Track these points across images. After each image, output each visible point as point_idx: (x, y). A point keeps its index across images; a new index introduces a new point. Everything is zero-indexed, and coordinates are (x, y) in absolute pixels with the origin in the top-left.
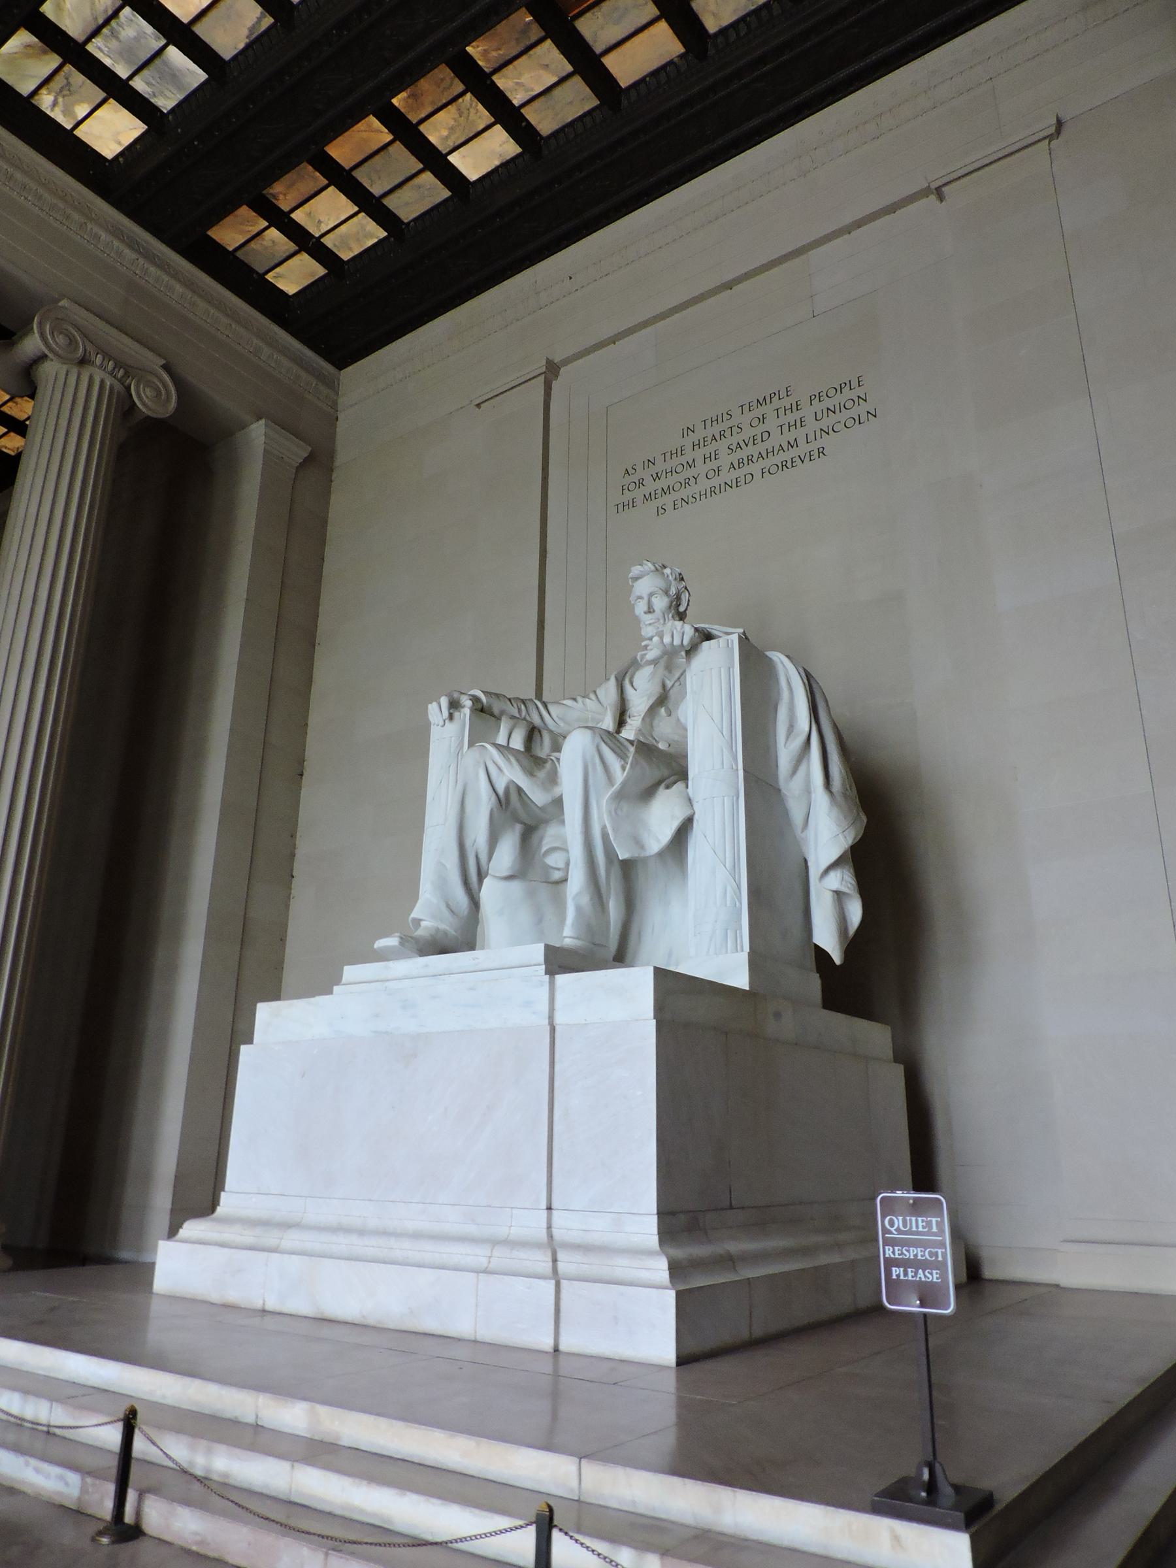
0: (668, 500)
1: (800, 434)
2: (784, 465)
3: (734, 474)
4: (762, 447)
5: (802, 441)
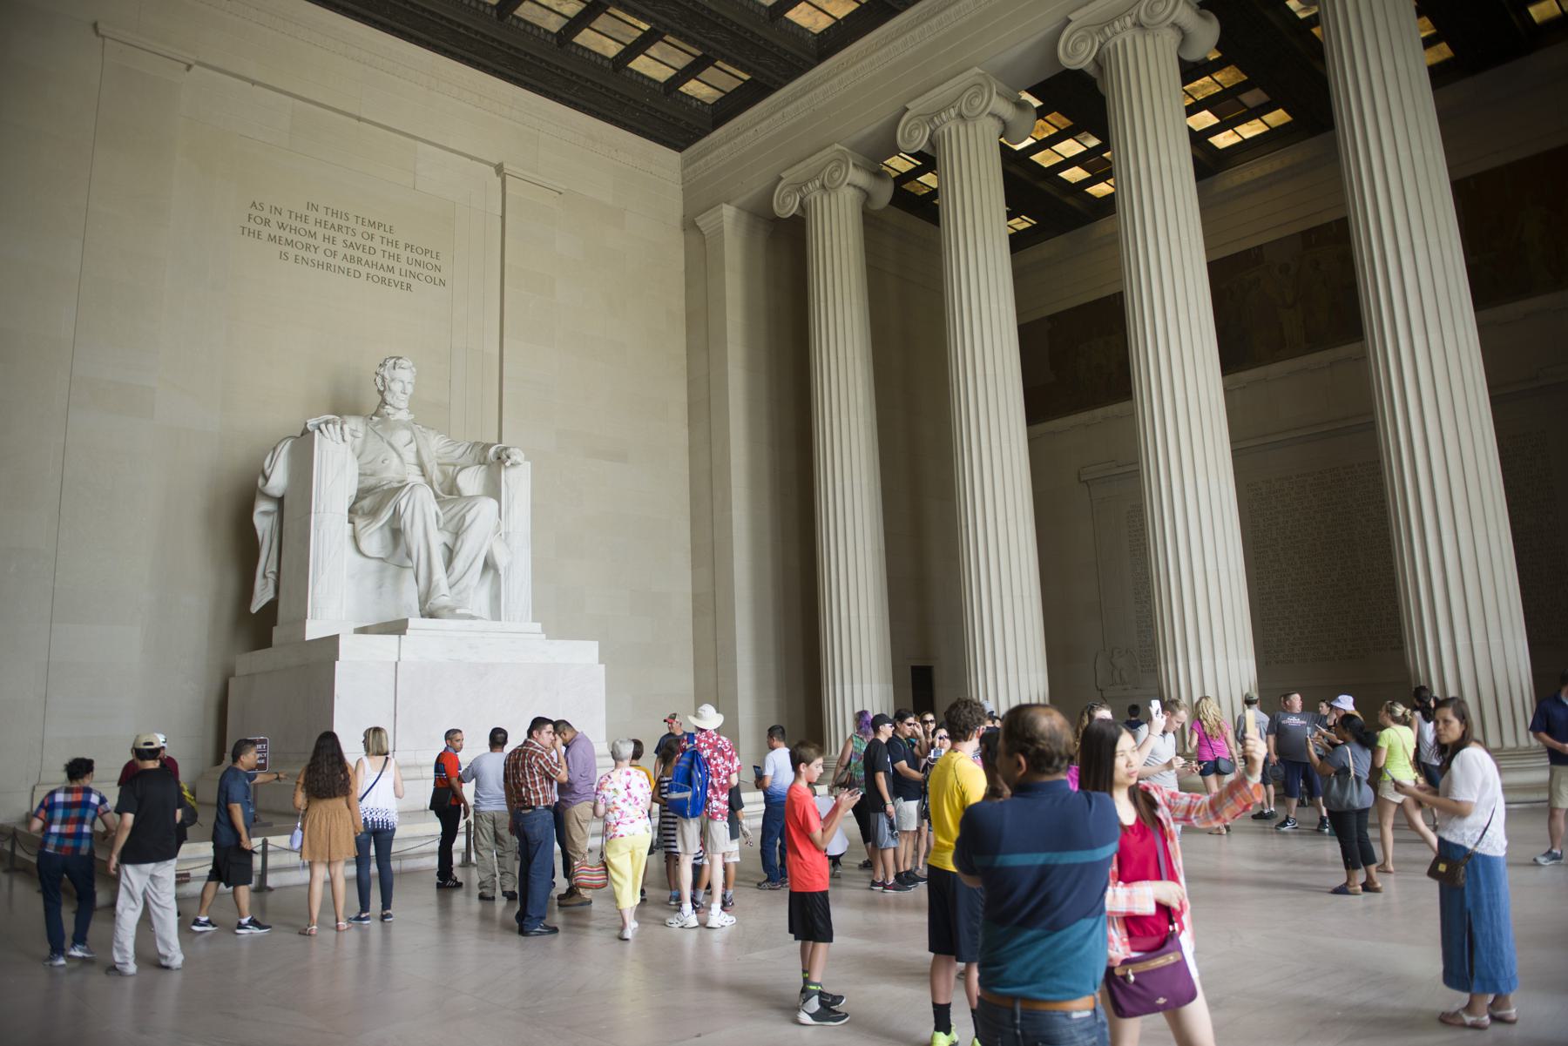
0: (292, 252)
1: (397, 266)
2: (383, 280)
3: (345, 265)
4: (370, 258)
5: (397, 271)
